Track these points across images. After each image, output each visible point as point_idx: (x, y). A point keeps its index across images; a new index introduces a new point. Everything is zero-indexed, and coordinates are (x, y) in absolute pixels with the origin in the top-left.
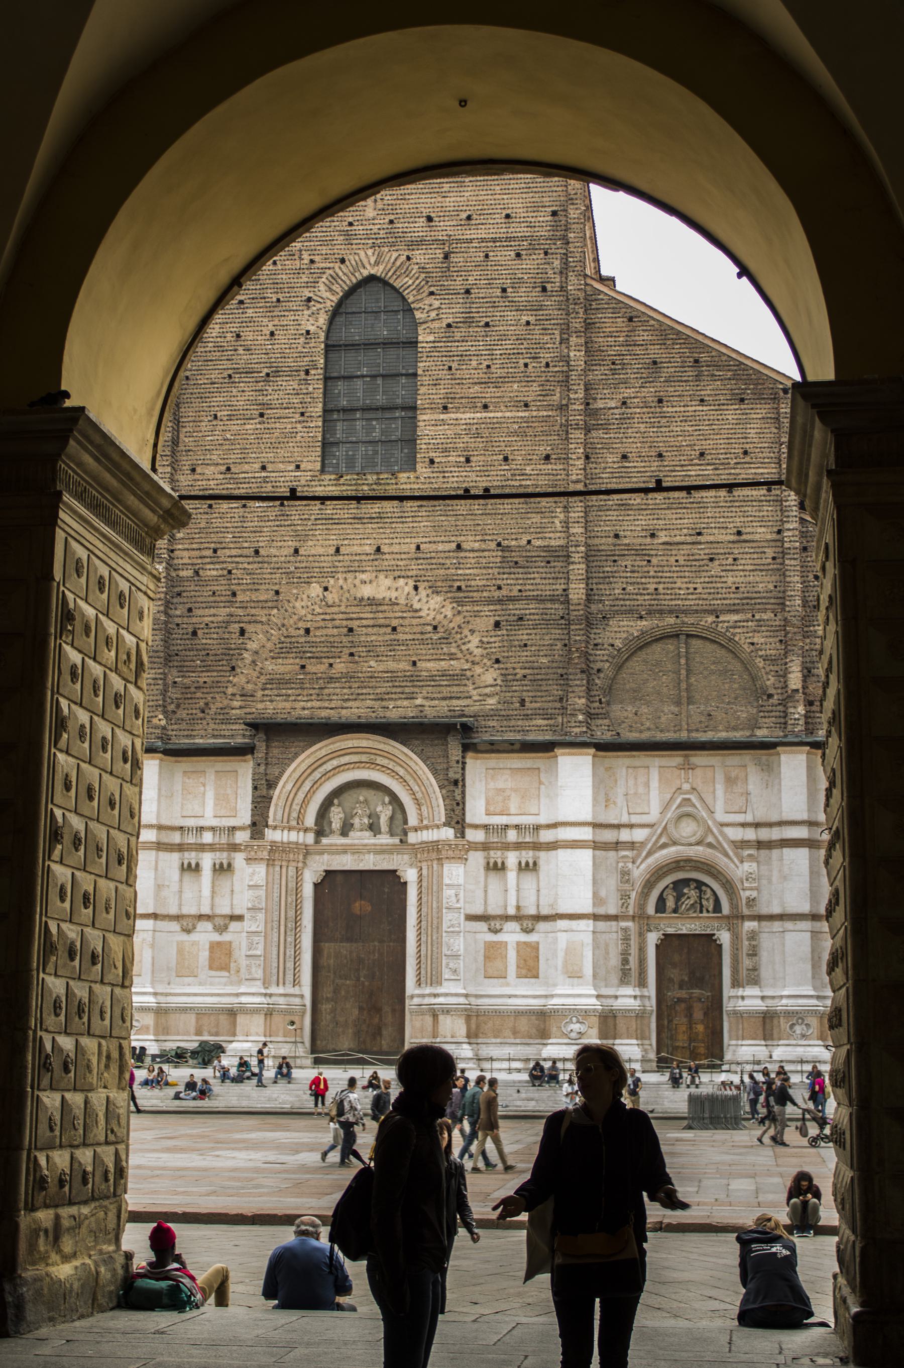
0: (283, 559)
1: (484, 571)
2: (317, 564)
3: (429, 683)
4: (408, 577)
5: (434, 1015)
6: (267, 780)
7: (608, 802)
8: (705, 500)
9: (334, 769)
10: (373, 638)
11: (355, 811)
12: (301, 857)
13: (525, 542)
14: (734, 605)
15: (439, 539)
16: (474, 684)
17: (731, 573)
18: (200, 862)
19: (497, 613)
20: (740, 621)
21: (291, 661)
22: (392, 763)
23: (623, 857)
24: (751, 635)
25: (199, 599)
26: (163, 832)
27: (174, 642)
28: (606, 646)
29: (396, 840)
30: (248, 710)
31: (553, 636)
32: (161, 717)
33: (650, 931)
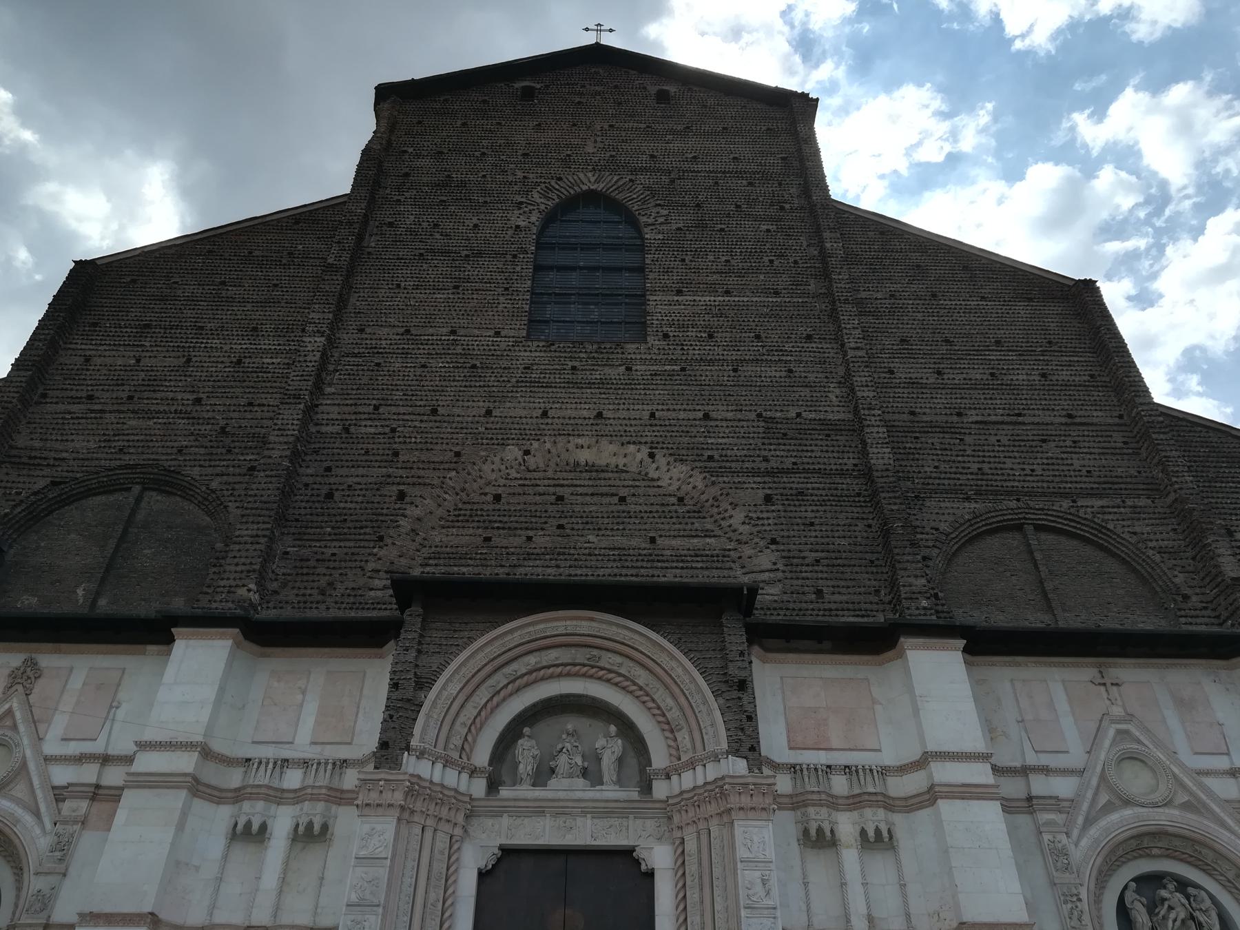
1: (744, 441)
2: (516, 426)
3: (675, 564)
4: (640, 443)
7: (991, 730)
8: (1014, 383)
9: (530, 673)
10: (593, 508)
11: (560, 746)
12: (460, 818)
13: (794, 415)
14: (1092, 488)
15: (679, 407)
16: (743, 567)
18: (269, 823)
20: (1108, 507)
21: (471, 531)
23: (1049, 823)
24: (1129, 523)
25: (343, 458)
31: (850, 515)
32: (252, 586)
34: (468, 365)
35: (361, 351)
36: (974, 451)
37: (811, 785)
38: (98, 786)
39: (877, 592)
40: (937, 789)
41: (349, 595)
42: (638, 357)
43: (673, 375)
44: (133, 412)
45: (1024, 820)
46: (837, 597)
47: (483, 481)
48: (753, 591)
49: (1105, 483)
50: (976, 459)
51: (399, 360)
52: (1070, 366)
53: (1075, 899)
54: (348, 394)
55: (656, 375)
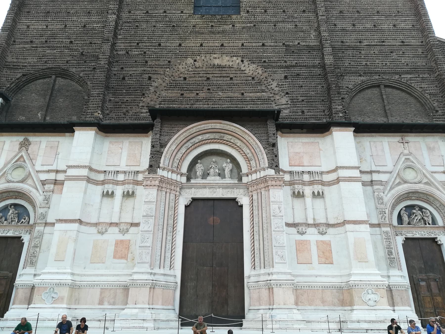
0: (173, 48)
1: (277, 55)
2: (191, 50)
3: (251, 103)
4: (238, 56)
5: (269, 288)
7: (361, 159)
8: (382, 29)
9: (199, 142)
10: (221, 82)
11: (211, 166)
12: (178, 189)
13: (297, 44)
14: (408, 71)
15: (253, 41)
16: (276, 103)
17: (402, 58)
19: (285, 72)
20: (413, 78)
21: (176, 91)
22: (233, 138)
23: (376, 189)
24: (420, 84)
25: (127, 64)
27: (112, 82)
28: (344, 88)
31: (316, 83)
32: (99, 112)
33: (397, 235)
34: (171, 26)
35: (130, 20)
36: (365, 57)
37: (296, 178)
38: (56, 180)
39: (324, 111)
40: (340, 178)
41: (134, 115)
42: (237, 21)
43: (251, 28)
44: (48, 47)
45: (369, 188)
46: (309, 114)
47: (179, 72)
48: (279, 112)
49: (413, 68)
50: (365, 60)
51: (145, 24)
52: (405, 21)
53: (384, 213)
54: (127, 38)
55: (244, 28)
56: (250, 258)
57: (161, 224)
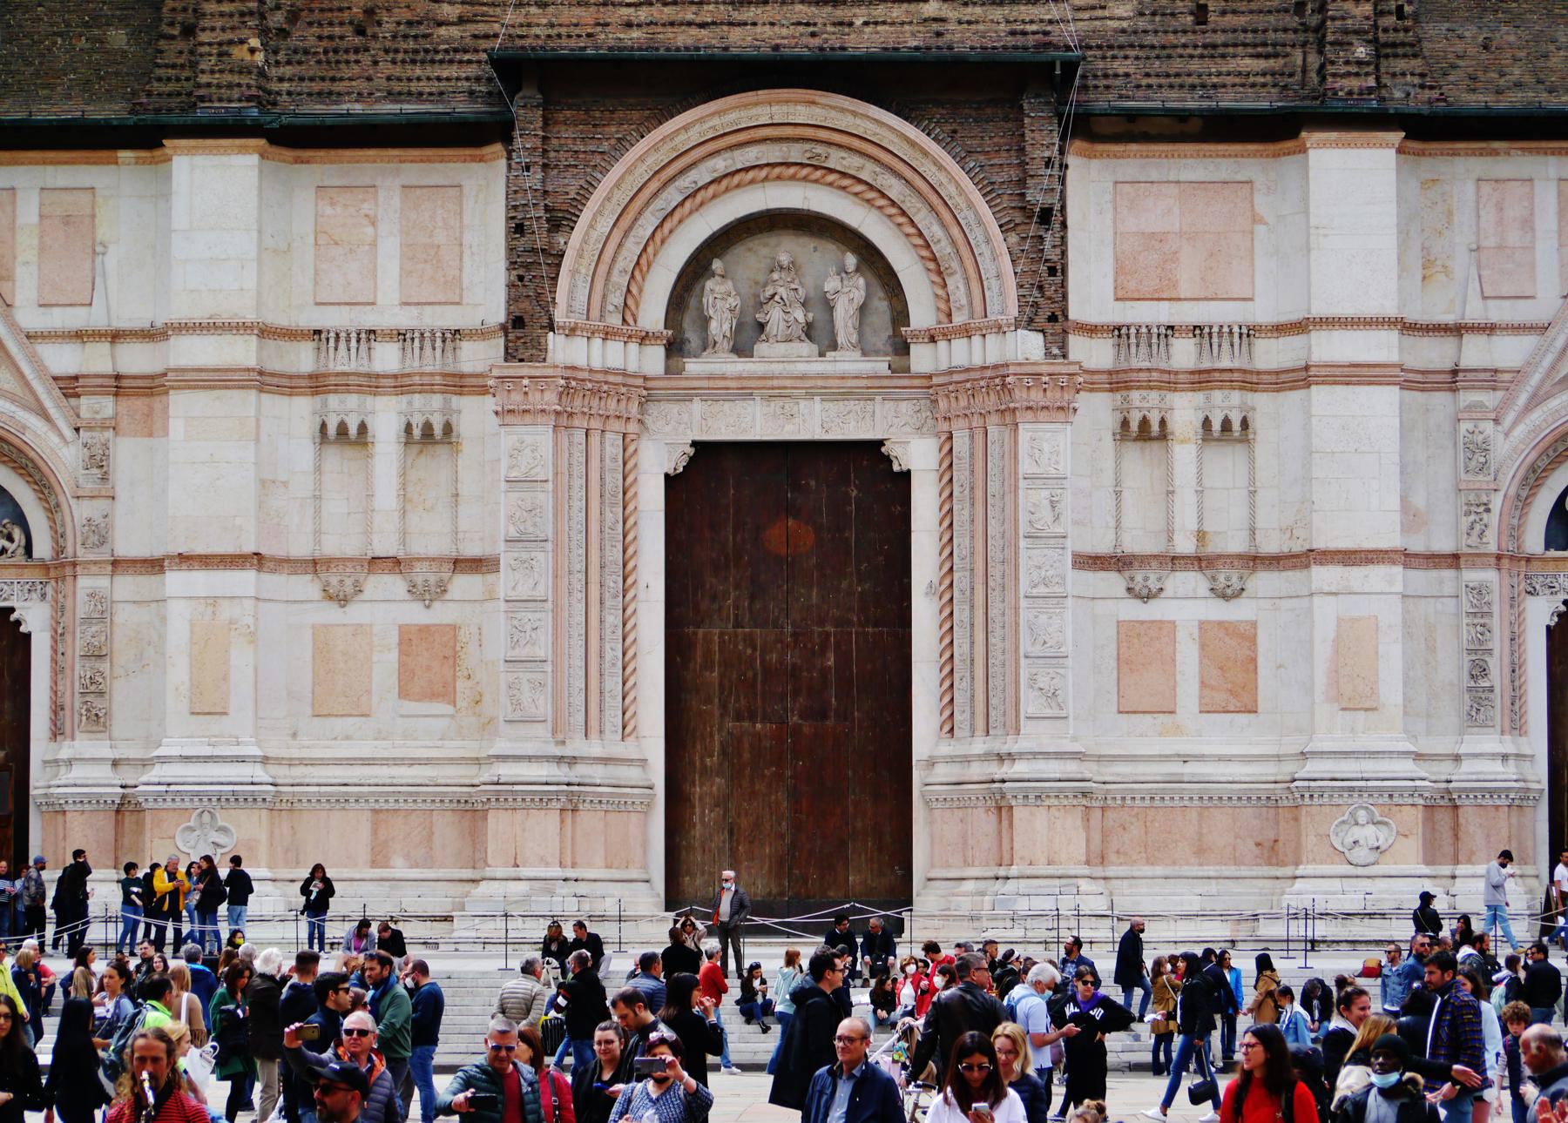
5: (1000, 808)
6: (547, 209)
7: (1430, 269)
12: (634, 409)
22: (870, 166)
23: (1470, 407)
26: (271, 344)
29: (881, 366)
30: (482, 28)
32: (255, 42)
33: (1532, 593)
37: (1139, 360)
38: (118, 377)
41: (406, 37)
53: (1481, 509)
56: (938, 692)
57: (578, 567)
